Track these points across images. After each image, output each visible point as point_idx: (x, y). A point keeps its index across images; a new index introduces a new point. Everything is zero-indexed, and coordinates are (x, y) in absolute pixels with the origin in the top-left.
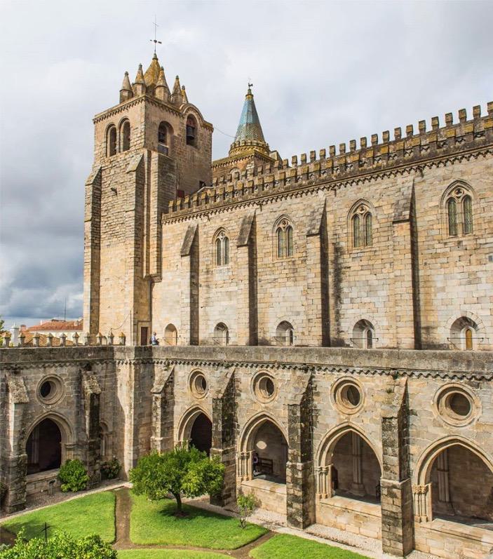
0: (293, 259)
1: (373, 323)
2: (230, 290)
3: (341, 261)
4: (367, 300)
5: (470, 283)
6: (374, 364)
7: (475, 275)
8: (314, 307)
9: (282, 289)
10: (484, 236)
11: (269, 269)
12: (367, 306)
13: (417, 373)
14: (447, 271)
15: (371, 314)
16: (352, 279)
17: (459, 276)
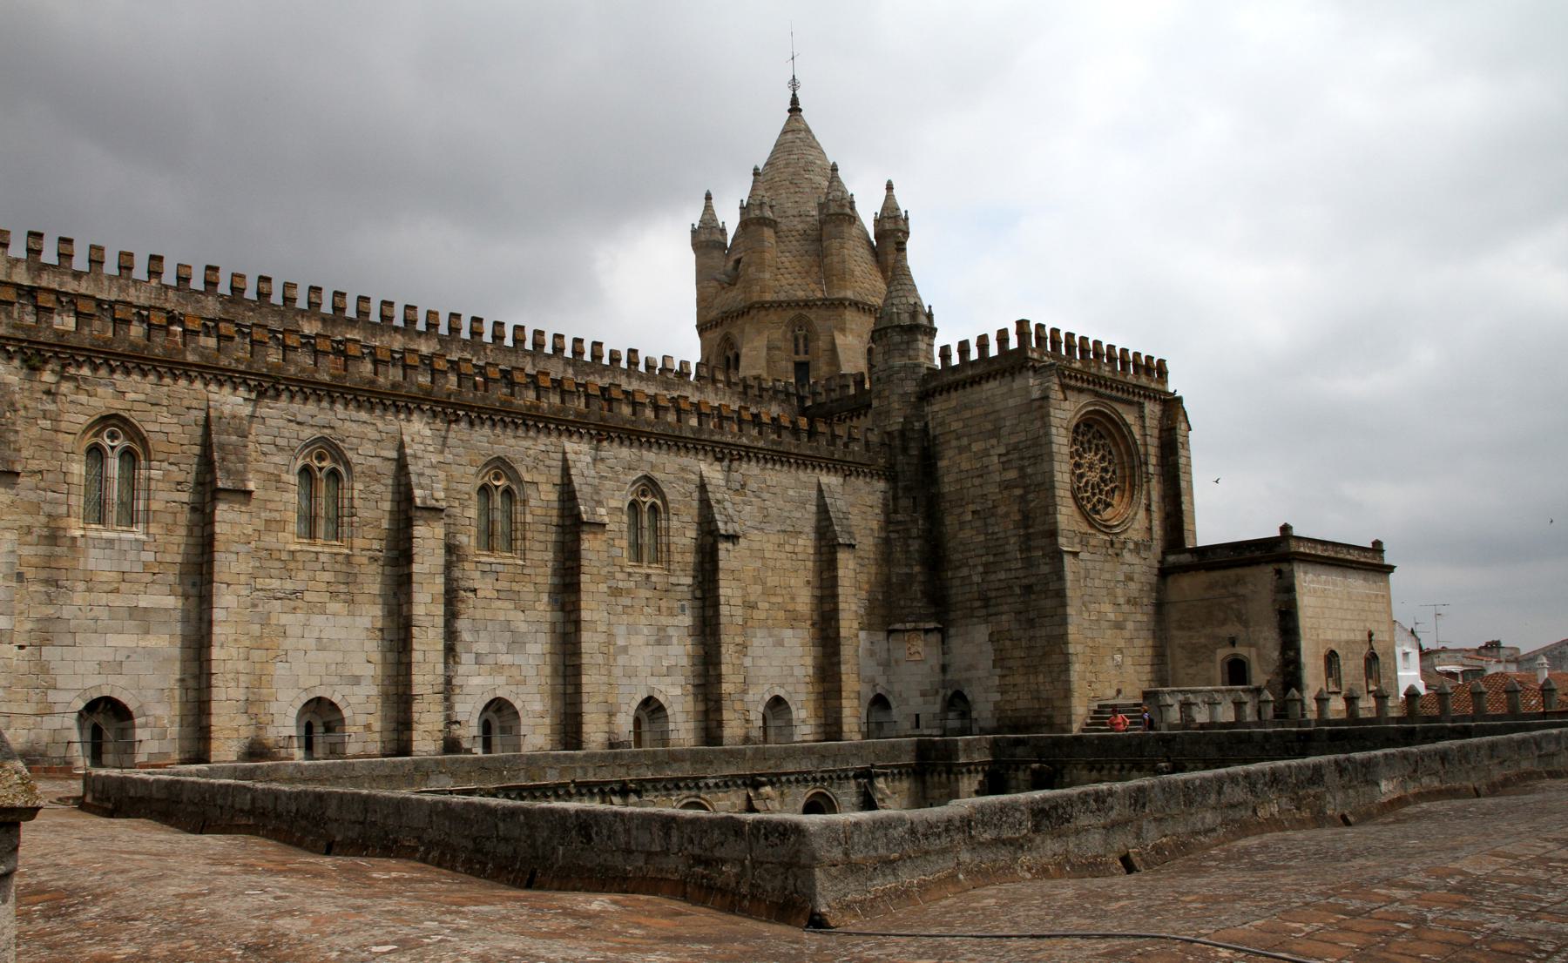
0: (346, 551)
1: (518, 705)
2: (142, 604)
3: (457, 573)
4: (505, 659)
5: (659, 643)
6: (732, 771)
7: (665, 631)
8: (428, 667)
9: (318, 620)
10: (678, 573)
11: (280, 565)
12: (507, 673)
13: (784, 779)
14: (631, 620)
15: (513, 688)
16: (479, 614)
17: (645, 631)
